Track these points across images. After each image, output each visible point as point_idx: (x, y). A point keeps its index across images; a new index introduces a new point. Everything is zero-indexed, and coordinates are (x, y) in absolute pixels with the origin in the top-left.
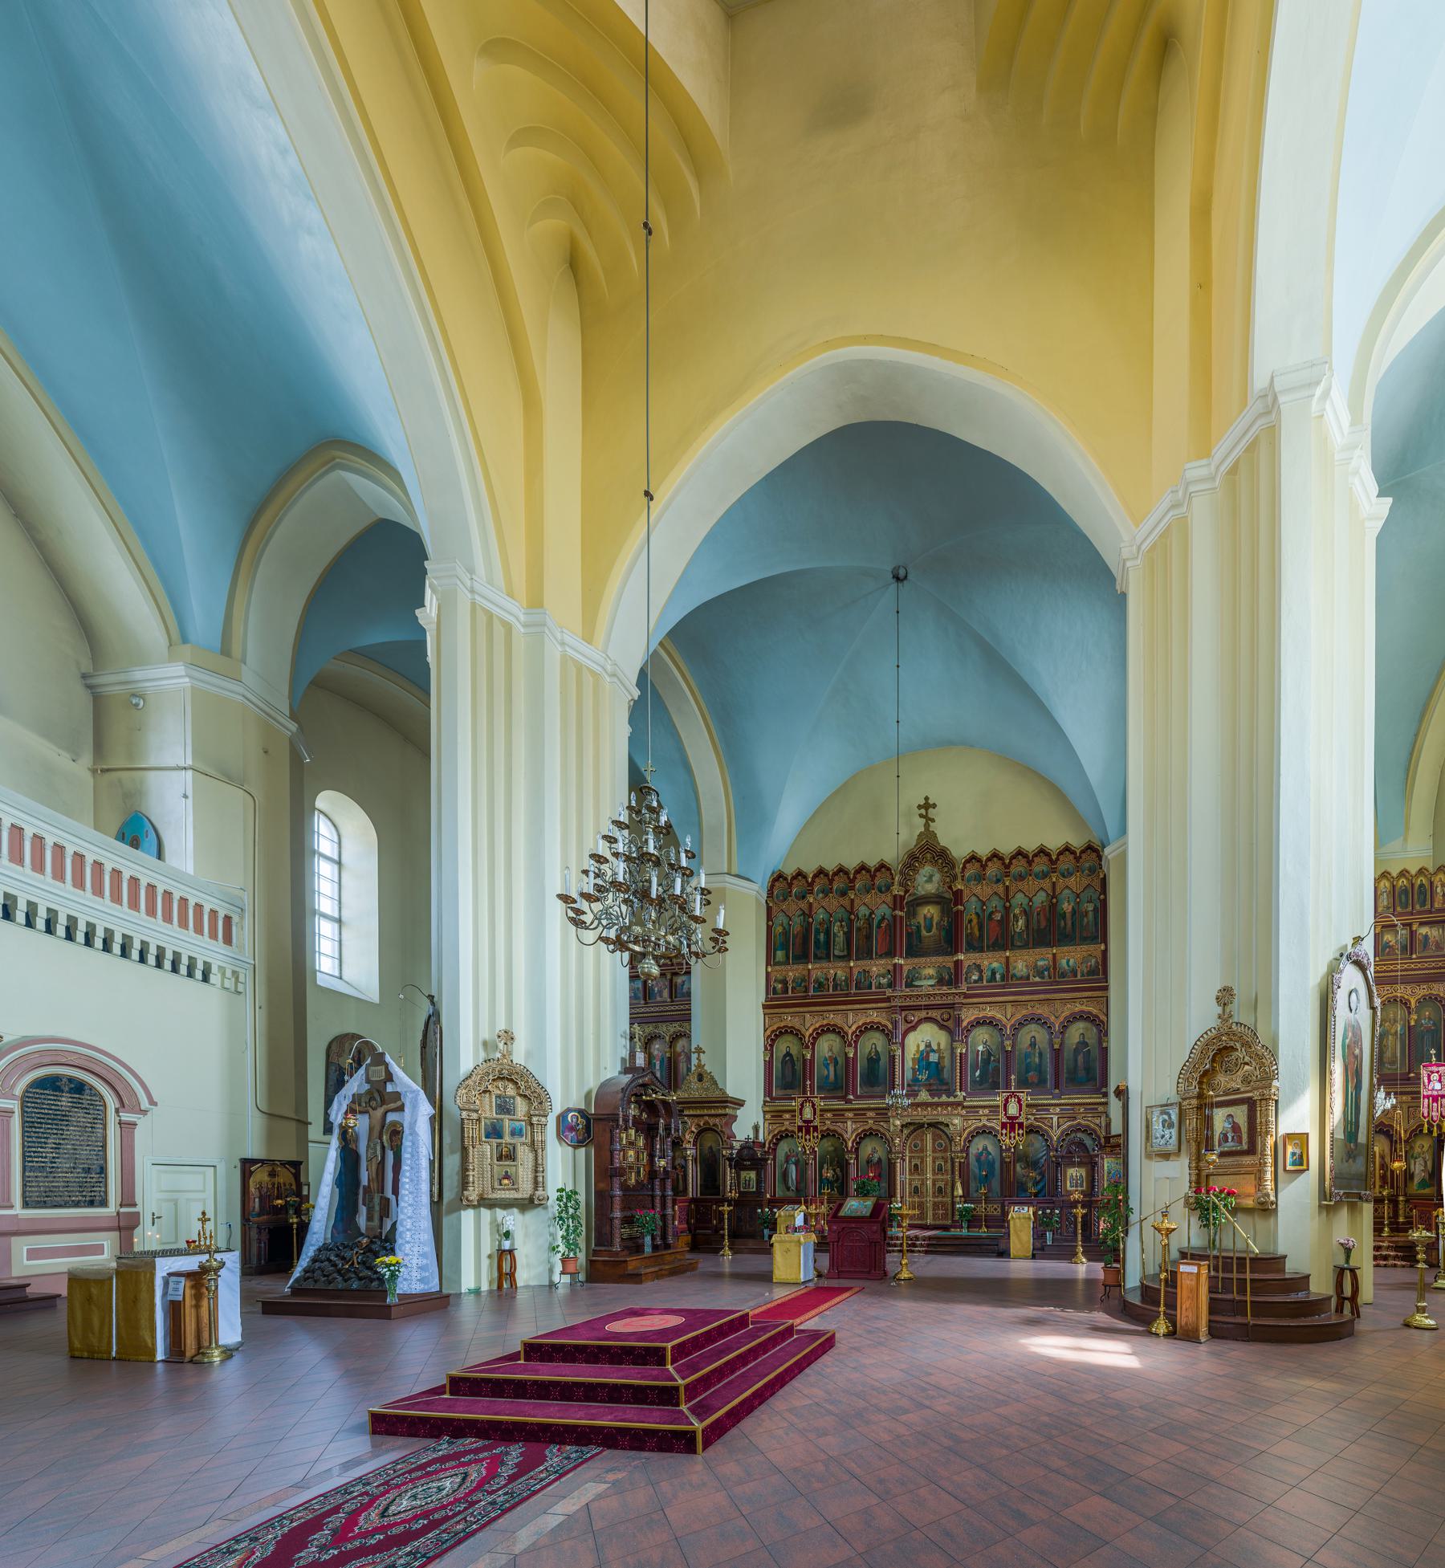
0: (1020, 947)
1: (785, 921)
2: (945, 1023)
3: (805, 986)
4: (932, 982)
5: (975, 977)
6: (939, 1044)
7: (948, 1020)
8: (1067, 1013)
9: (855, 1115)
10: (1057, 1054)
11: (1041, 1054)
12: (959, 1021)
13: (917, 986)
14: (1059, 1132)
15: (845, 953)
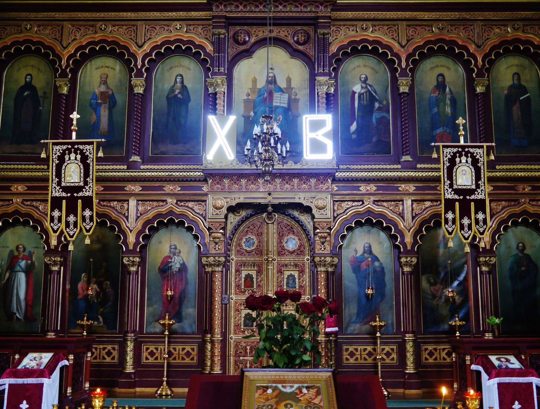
2: (300, 48)
6: (289, 80)
8: (494, 40)
9: (144, 188)
12: (324, 44)
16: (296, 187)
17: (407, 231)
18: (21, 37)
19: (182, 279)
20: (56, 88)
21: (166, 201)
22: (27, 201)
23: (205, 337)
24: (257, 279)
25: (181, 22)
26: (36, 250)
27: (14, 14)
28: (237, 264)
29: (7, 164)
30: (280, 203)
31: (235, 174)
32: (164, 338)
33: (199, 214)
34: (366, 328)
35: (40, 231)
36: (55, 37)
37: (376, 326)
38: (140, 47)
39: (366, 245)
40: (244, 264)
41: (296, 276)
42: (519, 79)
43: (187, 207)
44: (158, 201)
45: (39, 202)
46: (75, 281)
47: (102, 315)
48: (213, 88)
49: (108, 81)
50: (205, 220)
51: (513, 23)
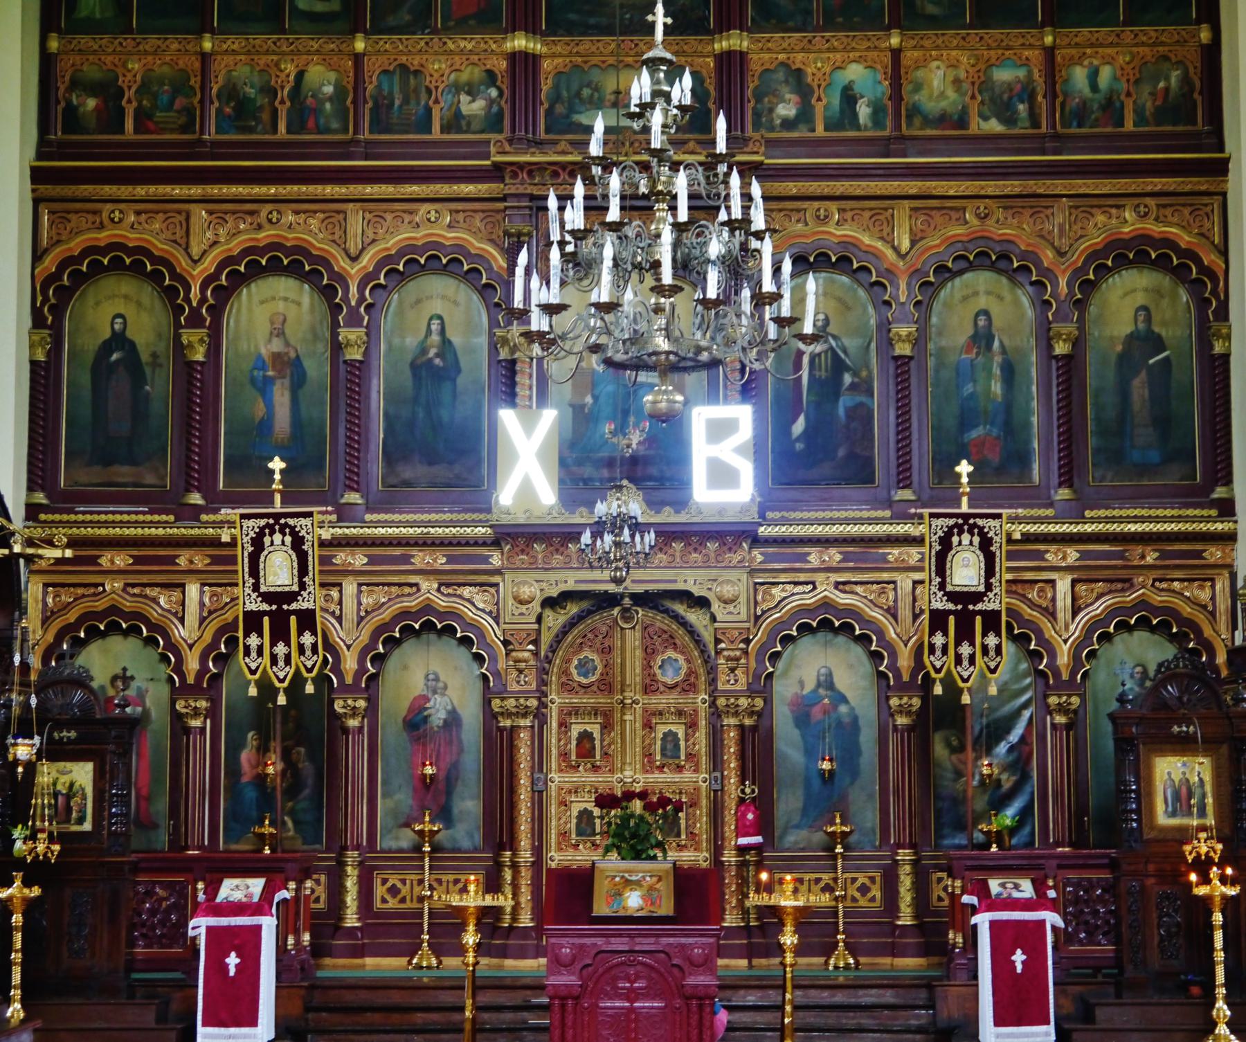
0: (933, 22)
3: (189, 112)
5: (786, 110)
8: (1096, 239)
9: (372, 560)
11: (1009, 372)
14: (1076, 629)
16: (678, 560)
17: (902, 645)
18: (104, 237)
19: (450, 743)
20: (179, 348)
22: (134, 586)
23: (500, 855)
24: (602, 741)
25: (437, 206)
26: (151, 686)
28: (561, 711)
29: (91, 513)
30: (647, 591)
31: (557, 535)
33: (483, 610)
34: (818, 837)
35: (164, 648)
36: (173, 238)
37: (834, 833)
38: (354, 259)
39: (823, 671)
40: (575, 711)
41: (681, 735)
42: (1148, 319)
43: (460, 597)
44: (400, 585)
45: (158, 589)
46: (235, 747)
47: (292, 813)
48: (506, 349)
49: (287, 331)
50: (498, 624)
51: (1136, 201)
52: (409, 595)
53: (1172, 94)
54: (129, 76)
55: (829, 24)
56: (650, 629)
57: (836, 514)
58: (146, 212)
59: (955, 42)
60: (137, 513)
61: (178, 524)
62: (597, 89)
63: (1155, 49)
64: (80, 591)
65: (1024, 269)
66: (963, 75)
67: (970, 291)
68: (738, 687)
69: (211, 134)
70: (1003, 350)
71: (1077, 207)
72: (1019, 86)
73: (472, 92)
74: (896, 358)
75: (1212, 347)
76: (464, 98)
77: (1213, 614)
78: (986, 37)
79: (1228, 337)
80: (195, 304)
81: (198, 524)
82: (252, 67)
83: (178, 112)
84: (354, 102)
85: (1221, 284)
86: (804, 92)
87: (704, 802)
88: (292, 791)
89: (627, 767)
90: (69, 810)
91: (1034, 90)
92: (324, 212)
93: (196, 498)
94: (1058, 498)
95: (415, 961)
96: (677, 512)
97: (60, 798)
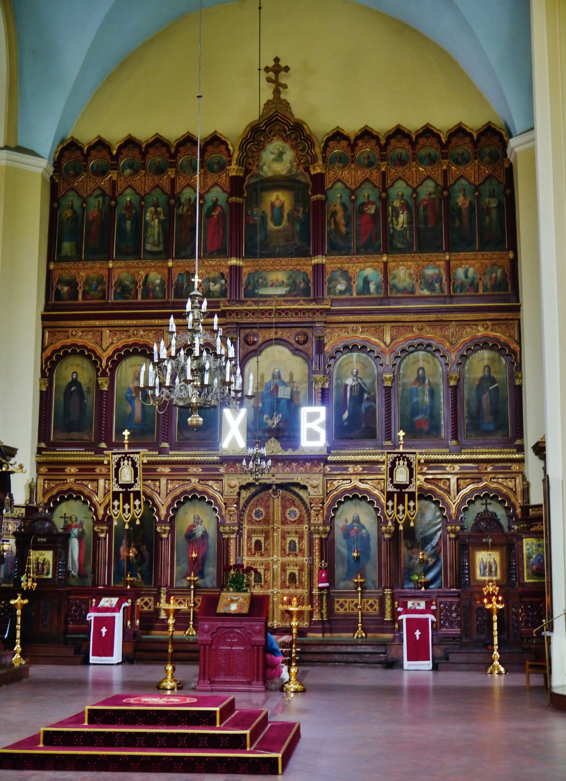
0: (401, 251)
1: (77, 203)
2: (300, 347)
3: (103, 291)
4: (282, 291)
5: (341, 287)
6: (291, 375)
7: (305, 342)
9: (173, 470)
10: (455, 391)
11: (432, 393)
12: (320, 345)
13: (261, 296)
14: (458, 499)
15: (161, 248)
18: (69, 342)
19: (204, 544)
20: (98, 385)
21: (190, 480)
22: (78, 480)
24: (265, 544)
26: (85, 520)
27: (63, 323)
28: (248, 531)
29: (62, 451)
32: (191, 591)
33: (216, 491)
35: (90, 505)
39: (355, 516)
40: (254, 532)
41: (297, 541)
42: (489, 371)
43: (208, 485)
44: (184, 480)
47: (140, 572)
51: (483, 323)
52: (187, 484)
53: (498, 280)
54: (81, 278)
55: (358, 252)
56: (285, 498)
57: (359, 451)
58: (85, 331)
59: (410, 259)
60: (80, 451)
61: (96, 455)
62: (265, 279)
63: (491, 261)
64: (58, 482)
65: (437, 350)
66: (412, 272)
67: (416, 360)
68: (319, 522)
69: (112, 300)
70: (430, 384)
71: (459, 325)
72: (436, 277)
73: (215, 281)
74: (385, 387)
75: (515, 382)
76: (211, 284)
77: (515, 492)
78: (422, 257)
79: (521, 378)
80: (104, 368)
81: (103, 455)
82: (128, 274)
83: (99, 291)
84: (168, 286)
85: (518, 356)
86: (349, 280)
87: (306, 569)
88: (141, 563)
89: (275, 555)
90: (43, 570)
91: (441, 278)
92: (155, 330)
93: (103, 445)
94: (451, 444)
95: (187, 633)
96: (294, 450)
97: (40, 565)
